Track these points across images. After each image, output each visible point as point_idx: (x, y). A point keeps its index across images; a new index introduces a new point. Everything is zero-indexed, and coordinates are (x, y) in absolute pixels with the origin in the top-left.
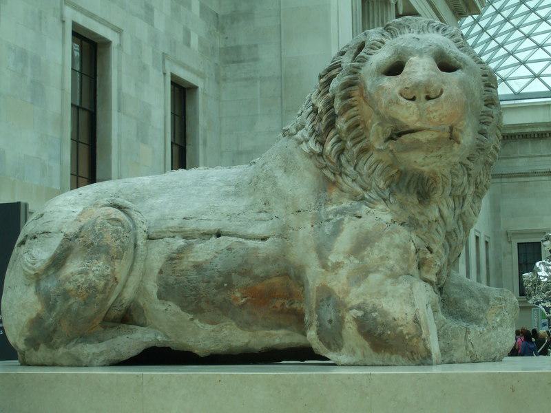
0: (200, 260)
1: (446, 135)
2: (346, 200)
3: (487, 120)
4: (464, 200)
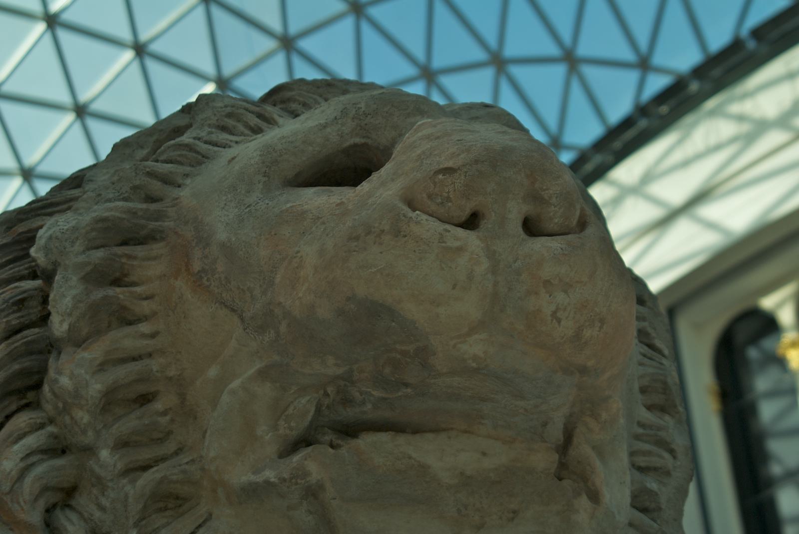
3: (655, 461)
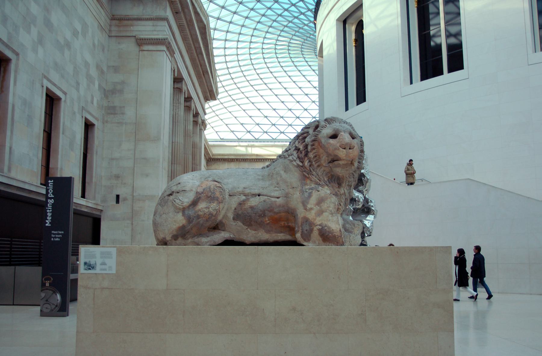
0: (253, 205)
1: (350, 162)
2: (313, 184)
4: (351, 187)
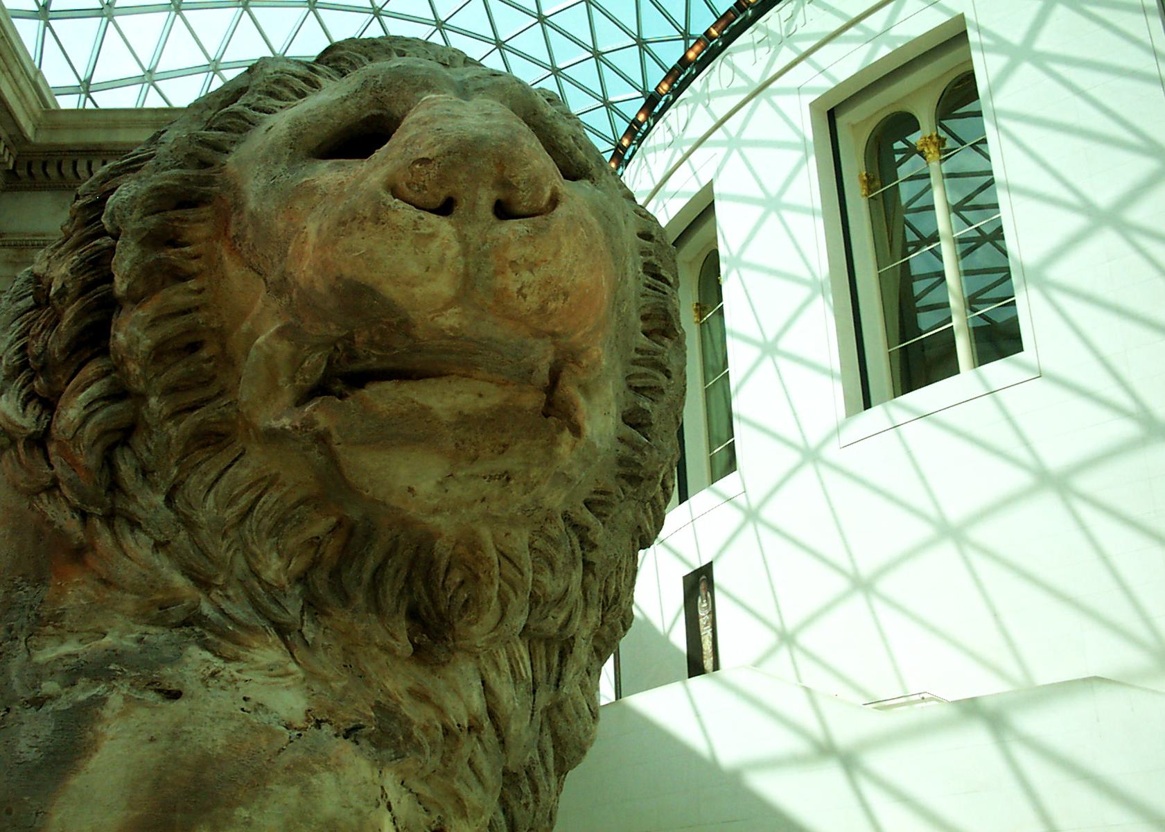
1: (532, 400)
3: (650, 382)
